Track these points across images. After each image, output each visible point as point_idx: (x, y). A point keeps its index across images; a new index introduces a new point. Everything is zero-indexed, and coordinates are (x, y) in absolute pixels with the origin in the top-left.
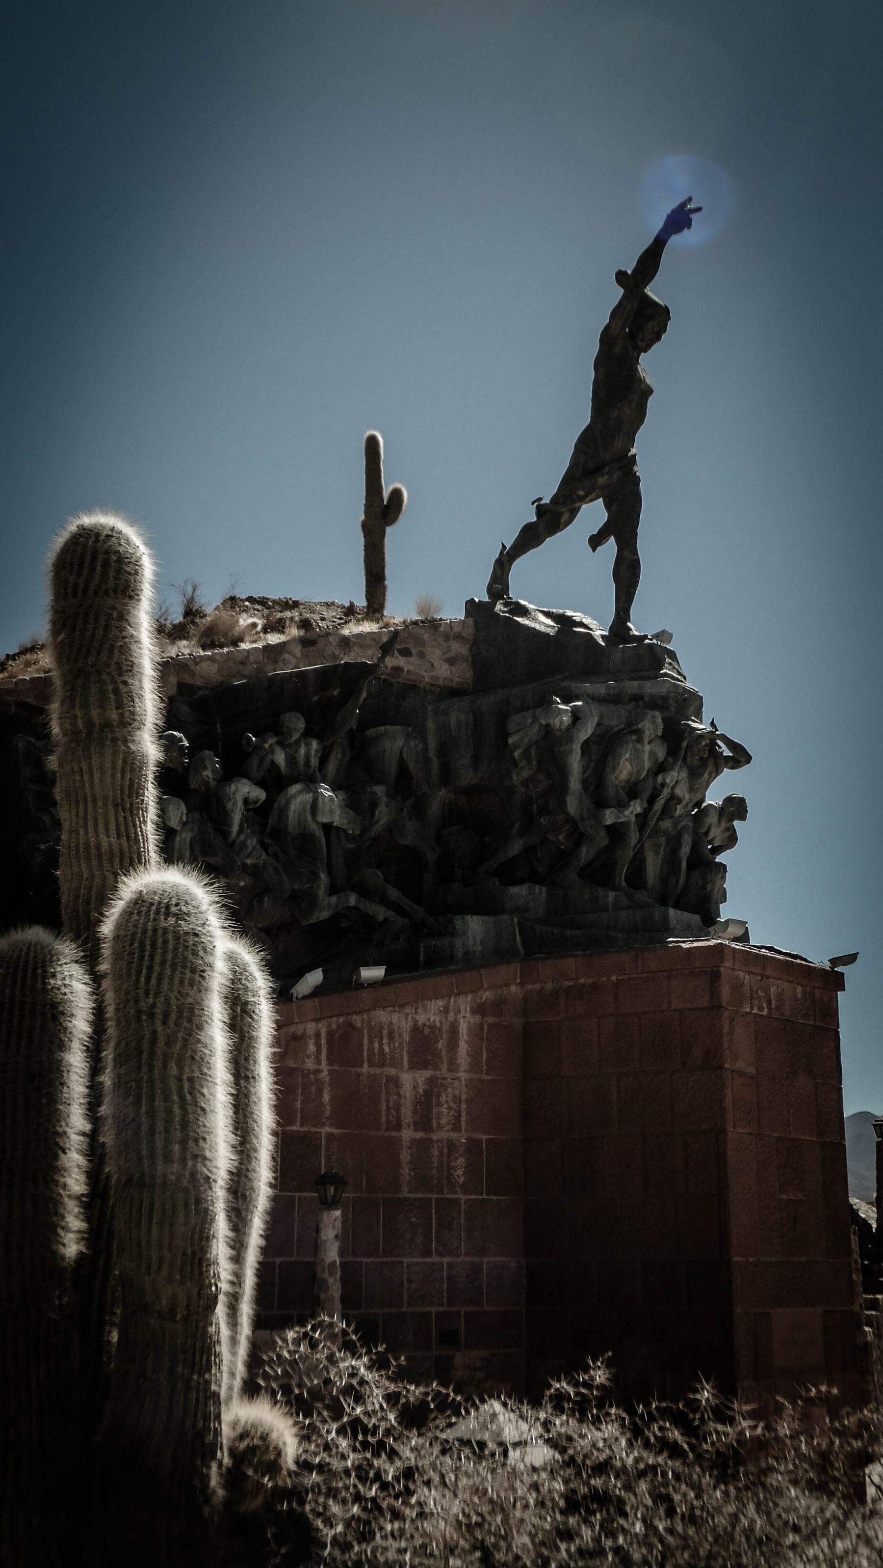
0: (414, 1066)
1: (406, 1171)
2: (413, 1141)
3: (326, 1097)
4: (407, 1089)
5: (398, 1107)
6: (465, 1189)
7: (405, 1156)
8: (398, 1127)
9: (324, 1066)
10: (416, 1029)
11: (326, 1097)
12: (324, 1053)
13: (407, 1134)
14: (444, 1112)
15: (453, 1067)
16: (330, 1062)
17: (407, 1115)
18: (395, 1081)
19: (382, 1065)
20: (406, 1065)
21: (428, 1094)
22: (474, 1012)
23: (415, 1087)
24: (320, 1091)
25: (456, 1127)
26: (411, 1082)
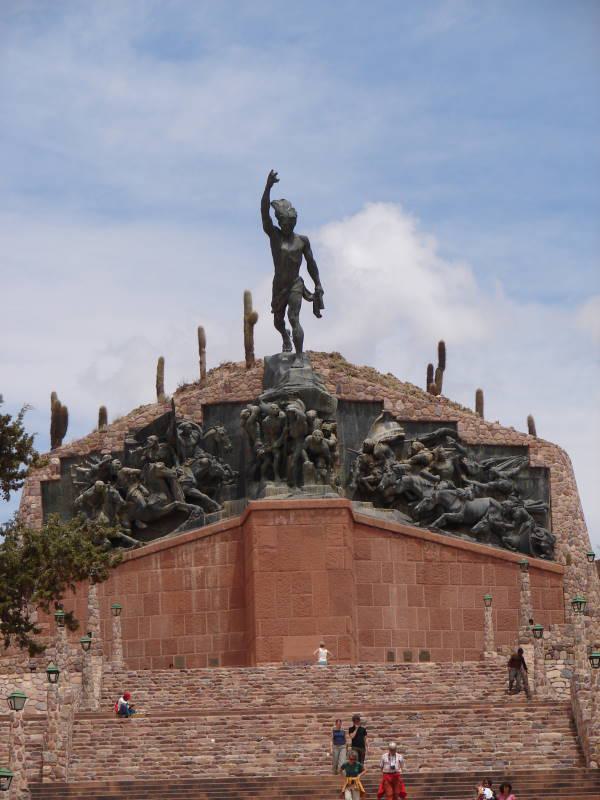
0: (196, 565)
1: (194, 604)
4: (194, 575)
7: (194, 598)
11: (160, 581)
13: (194, 591)
14: (210, 579)
17: (194, 584)
18: (189, 572)
19: (183, 566)
21: (203, 574)
24: (157, 580)
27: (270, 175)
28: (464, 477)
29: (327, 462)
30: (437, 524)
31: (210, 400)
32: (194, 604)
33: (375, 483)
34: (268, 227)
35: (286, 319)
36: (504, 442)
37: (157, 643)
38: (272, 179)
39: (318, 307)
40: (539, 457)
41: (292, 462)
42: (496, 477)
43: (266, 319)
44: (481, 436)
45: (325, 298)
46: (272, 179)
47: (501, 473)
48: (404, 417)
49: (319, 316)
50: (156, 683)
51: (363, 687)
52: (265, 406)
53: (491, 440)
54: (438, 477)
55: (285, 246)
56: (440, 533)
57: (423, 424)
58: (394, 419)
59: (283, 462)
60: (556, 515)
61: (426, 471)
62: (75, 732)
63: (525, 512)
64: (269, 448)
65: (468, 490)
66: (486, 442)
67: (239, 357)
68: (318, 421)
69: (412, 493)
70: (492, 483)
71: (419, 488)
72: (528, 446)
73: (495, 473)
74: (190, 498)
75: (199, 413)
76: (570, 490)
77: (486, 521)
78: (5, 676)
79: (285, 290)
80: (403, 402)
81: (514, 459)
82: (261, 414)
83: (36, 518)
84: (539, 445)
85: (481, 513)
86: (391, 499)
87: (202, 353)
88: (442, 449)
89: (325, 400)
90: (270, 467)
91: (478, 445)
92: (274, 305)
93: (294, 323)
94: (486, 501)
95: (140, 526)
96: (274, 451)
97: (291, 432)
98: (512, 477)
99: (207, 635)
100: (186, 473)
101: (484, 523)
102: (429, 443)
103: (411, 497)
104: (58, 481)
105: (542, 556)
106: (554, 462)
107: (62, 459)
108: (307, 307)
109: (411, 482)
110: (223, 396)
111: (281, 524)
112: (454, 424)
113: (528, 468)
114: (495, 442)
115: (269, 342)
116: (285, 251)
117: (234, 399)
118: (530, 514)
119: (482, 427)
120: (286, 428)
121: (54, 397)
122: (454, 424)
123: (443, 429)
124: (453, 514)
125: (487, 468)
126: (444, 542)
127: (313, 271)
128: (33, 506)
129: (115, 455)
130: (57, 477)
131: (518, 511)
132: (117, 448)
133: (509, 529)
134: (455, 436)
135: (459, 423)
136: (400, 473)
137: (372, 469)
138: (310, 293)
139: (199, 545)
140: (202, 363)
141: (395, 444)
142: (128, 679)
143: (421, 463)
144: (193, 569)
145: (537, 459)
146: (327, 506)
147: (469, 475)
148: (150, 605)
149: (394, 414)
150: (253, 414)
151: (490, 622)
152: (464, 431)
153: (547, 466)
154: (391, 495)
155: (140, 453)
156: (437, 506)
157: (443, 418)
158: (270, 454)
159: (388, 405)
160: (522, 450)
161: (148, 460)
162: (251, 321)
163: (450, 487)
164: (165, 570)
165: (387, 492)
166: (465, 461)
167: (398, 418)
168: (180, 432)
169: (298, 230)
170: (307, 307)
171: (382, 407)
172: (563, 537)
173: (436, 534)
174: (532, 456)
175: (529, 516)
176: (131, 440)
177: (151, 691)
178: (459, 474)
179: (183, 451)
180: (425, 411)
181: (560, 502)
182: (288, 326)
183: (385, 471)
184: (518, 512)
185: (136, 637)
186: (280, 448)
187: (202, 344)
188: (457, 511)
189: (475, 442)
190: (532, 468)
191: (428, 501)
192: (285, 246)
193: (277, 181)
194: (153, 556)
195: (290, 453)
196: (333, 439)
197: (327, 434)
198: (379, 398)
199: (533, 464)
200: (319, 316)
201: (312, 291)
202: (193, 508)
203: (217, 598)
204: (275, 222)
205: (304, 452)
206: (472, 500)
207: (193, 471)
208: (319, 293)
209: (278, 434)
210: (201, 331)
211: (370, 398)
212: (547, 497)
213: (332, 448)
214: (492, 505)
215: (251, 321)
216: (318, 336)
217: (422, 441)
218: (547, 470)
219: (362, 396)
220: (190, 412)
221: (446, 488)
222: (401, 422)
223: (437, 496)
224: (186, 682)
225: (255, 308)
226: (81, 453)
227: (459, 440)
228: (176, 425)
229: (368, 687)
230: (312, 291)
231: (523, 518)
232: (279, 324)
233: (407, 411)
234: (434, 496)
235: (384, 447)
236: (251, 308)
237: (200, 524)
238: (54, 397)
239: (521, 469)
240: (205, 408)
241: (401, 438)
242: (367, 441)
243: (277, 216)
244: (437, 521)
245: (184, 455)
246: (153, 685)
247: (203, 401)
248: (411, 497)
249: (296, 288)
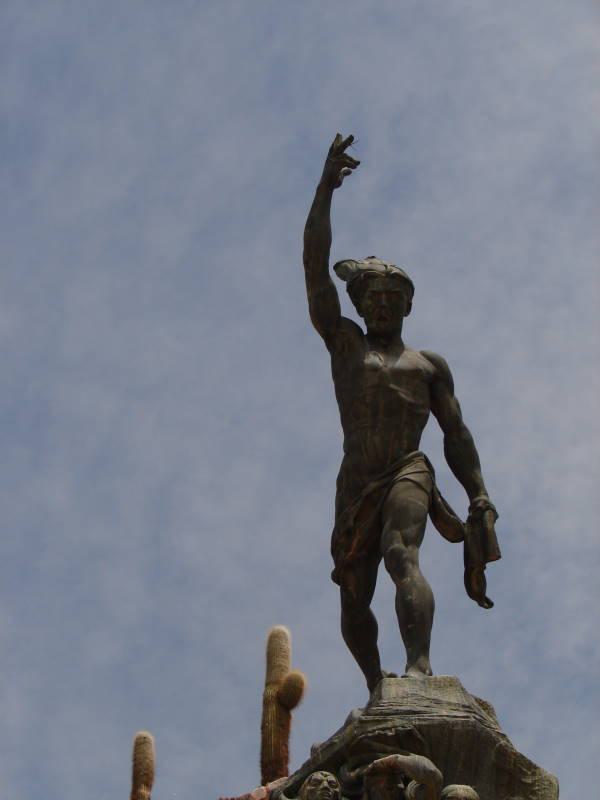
38: (339, 163)
39: (479, 543)
46: (339, 163)
49: (485, 603)
55: (374, 359)
79: (373, 485)
92: (340, 543)
108: (438, 561)
116: (375, 369)
127: (463, 457)
162: (284, 698)
170: (438, 561)
193: (355, 164)
200: (485, 603)
204: (348, 310)
208: (482, 513)
210: (140, 745)
215: (284, 698)
232: (359, 633)
236: (283, 669)
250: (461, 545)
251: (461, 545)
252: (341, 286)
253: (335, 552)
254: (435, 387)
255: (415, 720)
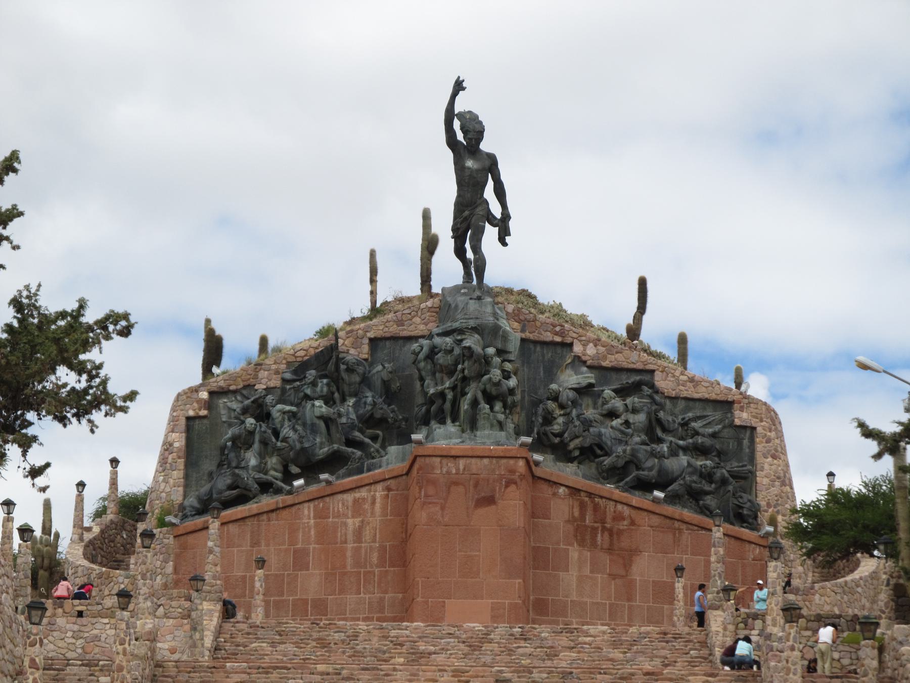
0: (353, 517)
1: (349, 561)
2: (353, 547)
3: (313, 532)
5: (346, 534)
6: (377, 566)
7: (349, 554)
8: (346, 542)
9: (312, 521)
10: (355, 498)
11: (313, 532)
12: (312, 515)
13: (350, 546)
14: (367, 534)
15: (372, 513)
16: (315, 518)
17: (350, 537)
18: (345, 524)
19: (338, 516)
20: (350, 515)
22: (383, 490)
23: (354, 524)
24: (309, 531)
25: (374, 541)
26: (352, 523)
27: (456, 82)
28: (659, 433)
29: (505, 406)
30: (627, 483)
31: (379, 334)
32: (349, 561)
33: (560, 435)
34: (452, 141)
35: (468, 245)
36: (707, 396)
37: (305, 601)
38: (459, 86)
40: (745, 415)
41: (465, 406)
42: (697, 433)
43: (446, 244)
44: (682, 388)
45: (512, 224)
46: (459, 86)
47: (701, 430)
48: (595, 363)
49: (504, 244)
50: (280, 635)
51: (520, 651)
52: (437, 340)
53: (689, 391)
54: (629, 431)
55: (470, 163)
56: (630, 493)
57: (617, 370)
58: (585, 362)
59: (455, 404)
60: (762, 479)
61: (616, 422)
62: (155, 676)
63: (727, 475)
64: (440, 388)
65: (665, 448)
66: (685, 394)
67: (413, 289)
68: (497, 360)
69: (601, 447)
70: (690, 441)
71: (609, 443)
72: (732, 403)
73: (694, 430)
74: (350, 443)
75: (366, 348)
76: (779, 453)
77: (682, 482)
78: (106, 621)
79: (467, 213)
80: (595, 346)
81: (718, 415)
82: (433, 351)
83: (179, 458)
84: (746, 401)
85: (676, 474)
86: (577, 453)
87: (373, 281)
88: (636, 399)
89: (505, 337)
90: (441, 410)
91: (674, 399)
92: (455, 229)
93: (477, 249)
94: (684, 459)
95: (293, 472)
96: (447, 391)
97: (466, 372)
98: (714, 435)
99: (362, 595)
100: (348, 410)
101: (681, 485)
102: (622, 392)
103: (599, 452)
104: (205, 417)
105: (745, 525)
106: (761, 421)
107: (211, 393)
108: (491, 233)
109: (600, 435)
110: (394, 330)
111: (449, 473)
112: (652, 372)
113: (732, 425)
114: (696, 396)
115: (448, 270)
116: (469, 168)
117: (405, 333)
118: (732, 476)
119: (682, 377)
120: (460, 367)
121: (208, 321)
122: (652, 372)
123: (638, 378)
124: (646, 473)
125: (685, 424)
126: (634, 503)
128: (176, 445)
129: (269, 390)
130: (204, 412)
131: (718, 474)
132: (272, 384)
133: (707, 493)
134: (652, 386)
135: (656, 373)
136: (587, 424)
137: (555, 419)
138: (495, 218)
139: (357, 495)
140: (373, 293)
141: (583, 391)
142: (247, 630)
143: (612, 414)
144: (350, 521)
145: (742, 417)
146: (502, 454)
147: (664, 430)
148: (300, 560)
149: (584, 358)
150: (424, 349)
151: (681, 596)
152: (660, 381)
153: (754, 425)
154: (574, 449)
155: (297, 390)
156: (627, 463)
157: (639, 366)
158: (442, 395)
159: (577, 348)
160: (726, 405)
161: (307, 397)
162: (430, 245)
163: (644, 443)
164: (318, 520)
165: (572, 445)
166: (661, 414)
167: (589, 363)
168: (343, 367)
169: (485, 146)
170: (491, 233)
171: (571, 350)
172: (769, 505)
173: (625, 494)
174: (737, 413)
175: (731, 479)
176: (288, 376)
177: (273, 644)
178: (654, 429)
179: (346, 388)
180: (619, 357)
181: (766, 466)
182: (470, 255)
183: (572, 421)
184: (718, 475)
185: (282, 595)
186: (453, 388)
187: (374, 272)
188: (650, 469)
189: (673, 394)
190: (737, 426)
191: (618, 457)
192: (470, 163)
193: (464, 89)
194: (306, 505)
195: (464, 394)
196: (512, 382)
197: (506, 375)
198: (569, 340)
199: (737, 422)
200: (504, 244)
201: (499, 216)
202: (353, 453)
203: (375, 555)
204: (460, 136)
205: (480, 396)
206: (667, 458)
207: (356, 412)
208: (506, 217)
209: (451, 373)
211: (558, 339)
212: (752, 459)
213: (511, 391)
214: (689, 465)
215: (430, 245)
216: (503, 265)
217: (614, 391)
218: (755, 428)
219: (548, 337)
220: (355, 345)
221: (637, 443)
222: (591, 367)
223: (628, 452)
224: (315, 635)
225: (434, 230)
226: (232, 388)
227: (657, 392)
228: (339, 360)
229: (528, 651)
230: (499, 216)
231: (724, 482)
232: (460, 252)
233: (597, 356)
234: (624, 451)
235: (572, 394)
237: (360, 471)
238: (208, 321)
239: (724, 427)
240: (373, 342)
241: (591, 385)
242: (554, 386)
243: (462, 129)
244: (628, 479)
245: (347, 393)
246: (278, 637)
247: (371, 335)
248: (599, 452)
249: (480, 211)
250: (497, 228)
251: (497, 228)
252: (457, 124)
253: (453, 230)
254: (491, 165)
255: (478, 322)
